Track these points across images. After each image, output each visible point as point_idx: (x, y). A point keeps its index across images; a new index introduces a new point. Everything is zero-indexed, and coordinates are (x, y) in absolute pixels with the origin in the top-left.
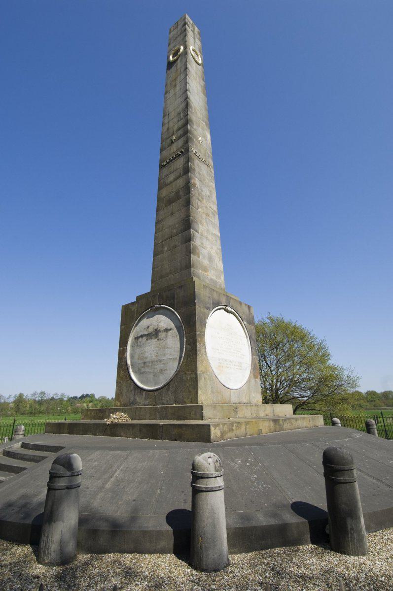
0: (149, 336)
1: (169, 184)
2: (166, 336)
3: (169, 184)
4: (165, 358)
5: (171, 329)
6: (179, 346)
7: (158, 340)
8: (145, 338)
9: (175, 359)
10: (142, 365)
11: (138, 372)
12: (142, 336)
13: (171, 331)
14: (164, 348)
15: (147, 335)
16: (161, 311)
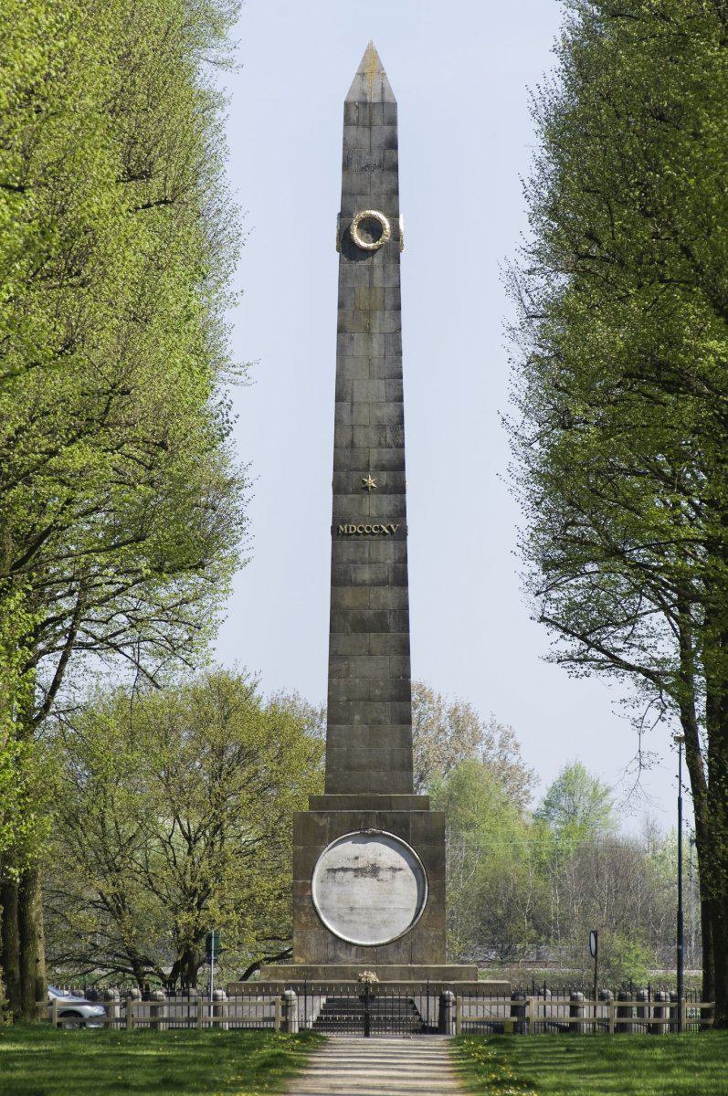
0: (359, 872)
1: (357, 585)
2: (393, 877)
3: (357, 585)
4: (392, 906)
5: (400, 869)
6: (415, 892)
7: (378, 880)
8: (350, 875)
9: (407, 910)
10: (347, 911)
11: (340, 919)
12: (345, 870)
13: (400, 872)
14: (391, 894)
15: (356, 870)
16: (381, 839)
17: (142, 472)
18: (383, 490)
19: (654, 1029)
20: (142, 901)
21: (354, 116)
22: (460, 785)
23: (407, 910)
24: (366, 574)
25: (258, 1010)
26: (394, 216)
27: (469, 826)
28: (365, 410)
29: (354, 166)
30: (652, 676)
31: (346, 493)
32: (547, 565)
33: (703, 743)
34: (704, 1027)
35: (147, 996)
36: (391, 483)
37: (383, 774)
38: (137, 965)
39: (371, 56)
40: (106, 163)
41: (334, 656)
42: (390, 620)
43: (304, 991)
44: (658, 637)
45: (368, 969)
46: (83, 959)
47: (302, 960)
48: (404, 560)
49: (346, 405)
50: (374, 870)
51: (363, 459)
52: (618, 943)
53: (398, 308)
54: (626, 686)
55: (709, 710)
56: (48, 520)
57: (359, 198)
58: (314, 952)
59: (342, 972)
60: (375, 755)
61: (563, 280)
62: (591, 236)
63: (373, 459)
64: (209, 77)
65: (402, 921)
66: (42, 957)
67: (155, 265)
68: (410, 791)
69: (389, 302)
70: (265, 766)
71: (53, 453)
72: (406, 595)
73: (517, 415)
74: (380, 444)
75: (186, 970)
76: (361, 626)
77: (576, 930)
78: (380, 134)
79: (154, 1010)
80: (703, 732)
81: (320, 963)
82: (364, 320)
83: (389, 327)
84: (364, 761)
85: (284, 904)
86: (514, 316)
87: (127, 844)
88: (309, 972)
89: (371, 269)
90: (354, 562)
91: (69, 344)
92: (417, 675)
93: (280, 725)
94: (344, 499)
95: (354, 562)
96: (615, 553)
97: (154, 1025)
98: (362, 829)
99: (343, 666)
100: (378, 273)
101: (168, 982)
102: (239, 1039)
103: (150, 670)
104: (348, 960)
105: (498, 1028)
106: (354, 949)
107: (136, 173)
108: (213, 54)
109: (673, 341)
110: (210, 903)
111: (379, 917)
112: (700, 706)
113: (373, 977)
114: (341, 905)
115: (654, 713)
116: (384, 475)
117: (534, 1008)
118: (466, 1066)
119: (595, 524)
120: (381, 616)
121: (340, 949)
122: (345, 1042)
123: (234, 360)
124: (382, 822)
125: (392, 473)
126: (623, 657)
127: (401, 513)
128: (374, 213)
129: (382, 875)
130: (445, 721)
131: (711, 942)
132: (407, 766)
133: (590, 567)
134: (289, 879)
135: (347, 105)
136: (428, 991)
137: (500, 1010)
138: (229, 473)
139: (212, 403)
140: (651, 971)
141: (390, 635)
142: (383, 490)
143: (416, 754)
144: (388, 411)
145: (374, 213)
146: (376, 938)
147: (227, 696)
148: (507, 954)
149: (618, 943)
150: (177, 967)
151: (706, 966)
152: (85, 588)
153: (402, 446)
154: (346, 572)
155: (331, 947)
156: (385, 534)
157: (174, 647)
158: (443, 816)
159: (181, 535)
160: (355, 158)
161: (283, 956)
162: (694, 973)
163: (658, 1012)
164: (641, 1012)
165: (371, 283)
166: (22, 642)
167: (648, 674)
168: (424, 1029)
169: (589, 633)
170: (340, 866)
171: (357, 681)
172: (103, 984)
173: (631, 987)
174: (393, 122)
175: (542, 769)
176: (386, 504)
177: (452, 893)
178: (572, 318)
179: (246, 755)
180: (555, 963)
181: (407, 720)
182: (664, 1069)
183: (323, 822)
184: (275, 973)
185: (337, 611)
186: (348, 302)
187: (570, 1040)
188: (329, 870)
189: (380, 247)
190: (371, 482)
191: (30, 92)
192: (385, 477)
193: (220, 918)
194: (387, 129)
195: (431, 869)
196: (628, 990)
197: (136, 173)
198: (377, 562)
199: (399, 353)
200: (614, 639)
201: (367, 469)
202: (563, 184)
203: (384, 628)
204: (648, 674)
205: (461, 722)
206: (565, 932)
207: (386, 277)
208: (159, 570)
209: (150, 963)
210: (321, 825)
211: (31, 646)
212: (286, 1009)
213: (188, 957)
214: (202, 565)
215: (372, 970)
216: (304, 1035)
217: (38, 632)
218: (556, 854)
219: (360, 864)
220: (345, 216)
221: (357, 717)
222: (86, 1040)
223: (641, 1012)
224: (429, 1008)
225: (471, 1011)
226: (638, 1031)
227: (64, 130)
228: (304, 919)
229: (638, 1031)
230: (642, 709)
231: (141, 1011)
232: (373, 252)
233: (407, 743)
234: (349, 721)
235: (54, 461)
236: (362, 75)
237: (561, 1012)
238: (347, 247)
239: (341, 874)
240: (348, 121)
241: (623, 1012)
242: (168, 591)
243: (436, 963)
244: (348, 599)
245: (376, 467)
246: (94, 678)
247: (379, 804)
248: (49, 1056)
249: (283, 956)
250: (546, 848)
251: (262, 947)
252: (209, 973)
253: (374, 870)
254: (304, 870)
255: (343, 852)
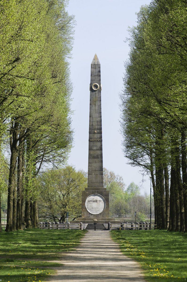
2: (100, 202)
6: (104, 205)
8: (92, 202)
11: (90, 210)
12: (91, 201)
17: (55, 130)
18: (98, 133)
19: (146, 229)
20: (55, 207)
21: (93, 67)
22: (112, 186)
23: (103, 208)
24: (95, 148)
25: (76, 226)
26: (100, 84)
27: (113, 193)
28: (95, 119)
29: (93, 75)
30: (146, 166)
31: (91, 134)
32: (127, 147)
33: (155, 178)
34: (155, 229)
35: (56, 223)
36: (99, 132)
37: (98, 184)
38: (54, 218)
39: (96, 56)
40: (48, 74)
41: (89, 163)
42: (99, 157)
43: (84, 222)
44: (147, 159)
45: (95, 219)
46: (45, 217)
47: (84, 217)
48: (102, 146)
49: (91, 118)
50: (96, 201)
51: (94, 128)
52: (140, 214)
53: (101, 101)
54: (141, 168)
55: (156, 173)
56: (39, 138)
57: (94, 81)
58: (86, 216)
59: (91, 219)
60: (97, 182)
61: (129, 96)
62: (135, 88)
63: (96, 127)
64: (67, 60)
65: (101, 210)
66: (37, 216)
67: (57, 93)
68: (103, 187)
69: (99, 99)
70: (77, 183)
71: (39, 126)
72: (102, 152)
73: (122, 121)
74: (97, 125)
75: (63, 219)
76: (94, 157)
77: (132, 212)
78: (97, 70)
79: (57, 226)
80: (155, 176)
81: (87, 217)
82: (94, 103)
83: (99, 104)
84: (95, 182)
85: (80, 207)
86: (121, 102)
87: (52, 196)
88: (85, 219)
89: (96, 94)
90: (93, 146)
91: (42, 107)
92: (104, 166)
93: (80, 175)
94: (91, 135)
95: (93, 146)
96: (139, 144)
97: (57, 228)
98: (94, 194)
99: (91, 165)
100: (97, 94)
101: (60, 221)
102: (73, 231)
103: (56, 165)
104: (92, 217)
105: (118, 229)
106: (93, 215)
107: (54, 77)
108: (68, 56)
109: (149, 107)
110: (67, 207)
111: (97, 209)
112: (154, 172)
113: (96, 220)
114: (91, 207)
115: (146, 173)
116: (98, 130)
117: (125, 226)
118: (113, 235)
119: (136, 139)
120: (98, 156)
121: (90, 215)
122: (91, 231)
123: (71, 110)
124: (98, 192)
125: (99, 130)
126: (141, 163)
127: (101, 137)
128: (96, 84)
129: (98, 202)
130: (109, 174)
131: (156, 214)
132: (102, 182)
133: (135, 147)
134: (81, 203)
135: (91, 64)
136: (106, 222)
137: (118, 226)
138: (71, 130)
139: (68, 117)
140: (145, 219)
141: (99, 159)
142: (98, 133)
143: (104, 180)
144: (99, 119)
145: (96, 84)
146: (97, 213)
147: (70, 170)
148: (120, 216)
149: (140, 214)
150: (61, 218)
151: (155, 218)
152: (45, 151)
153: (101, 125)
154: (91, 148)
155: (89, 215)
156: (98, 141)
157: (60, 161)
158: (109, 191)
159: (62, 141)
160: (93, 74)
161: (80, 216)
162: (153, 219)
163: (147, 226)
164: (144, 226)
165: (96, 96)
166: (34, 161)
167: (145, 166)
168: (105, 229)
169: (134, 159)
170: (90, 200)
171: (93, 167)
172: (48, 221)
173: (142, 222)
174: (100, 68)
175: (127, 183)
176: (99, 135)
177: (110, 205)
178: (132, 103)
179: (73, 181)
180: (129, 217)
181: (102, 174)
182: (148, 236)
183: (87, 192)
184: (79, 219)
185: (90, 155)
186: (92, 100)
187: (131, 231)
188: (88, 201)
189: (97, 90)
190: (96, 132)
191: (35, 62)
192: (98, 131)
193: (69, 209)
194: (99, 69)
195: (107, 201)
196: (141, 223)
197: (54, 77)
198: (97, 146)
199: (101, 109)
200: (139, 160)
201: (95, 129)
202: (130, 78)
203: (98, 158)
204: (145, 166)
205: (112, 175)
206: (130, 212)
207: (98, 95)
208: (58, 147)
209: (56, 218)
210: (87, 193)
211: (35, 161)
212: (81, 226)
213: (63, 216)
214: (66, 147)
215: (97, 219)
216: (84, 230)
217: (36, 159)
218: (129, 198)
219: (94, 200)
220: (91, 84)
221: (93, 174)
222: (45, 231)
223: (144, 226)
224: (106, 226)
225: (113, 226)
226: (143, 229)
227: (40, 69)
228: (84, 210)
229: (143, 229)
230: (144, 172)
231: (55, 226)
232: (96, 91)
233: (102, 178)
234: (92, 174)
235: (39, 128)
236: (94, 59)
237: (130, 226)
238: (91, 89)
239: (90, 202)
240: (92, 68)
241: (140, 226)
242: (59, 152)
243: (107, 217)
244: (92, 153)
245: (97, 129)
246: (46, 167)
247: (97, 189)
248: (39, 234)
249: (80, 216)
250: (127, 197)
251: (76, 215)
252: (67, 219)
253: (96, 201)
254: (84, 201)
255: (91, 198)
